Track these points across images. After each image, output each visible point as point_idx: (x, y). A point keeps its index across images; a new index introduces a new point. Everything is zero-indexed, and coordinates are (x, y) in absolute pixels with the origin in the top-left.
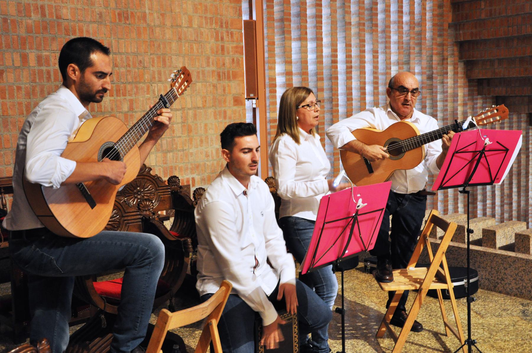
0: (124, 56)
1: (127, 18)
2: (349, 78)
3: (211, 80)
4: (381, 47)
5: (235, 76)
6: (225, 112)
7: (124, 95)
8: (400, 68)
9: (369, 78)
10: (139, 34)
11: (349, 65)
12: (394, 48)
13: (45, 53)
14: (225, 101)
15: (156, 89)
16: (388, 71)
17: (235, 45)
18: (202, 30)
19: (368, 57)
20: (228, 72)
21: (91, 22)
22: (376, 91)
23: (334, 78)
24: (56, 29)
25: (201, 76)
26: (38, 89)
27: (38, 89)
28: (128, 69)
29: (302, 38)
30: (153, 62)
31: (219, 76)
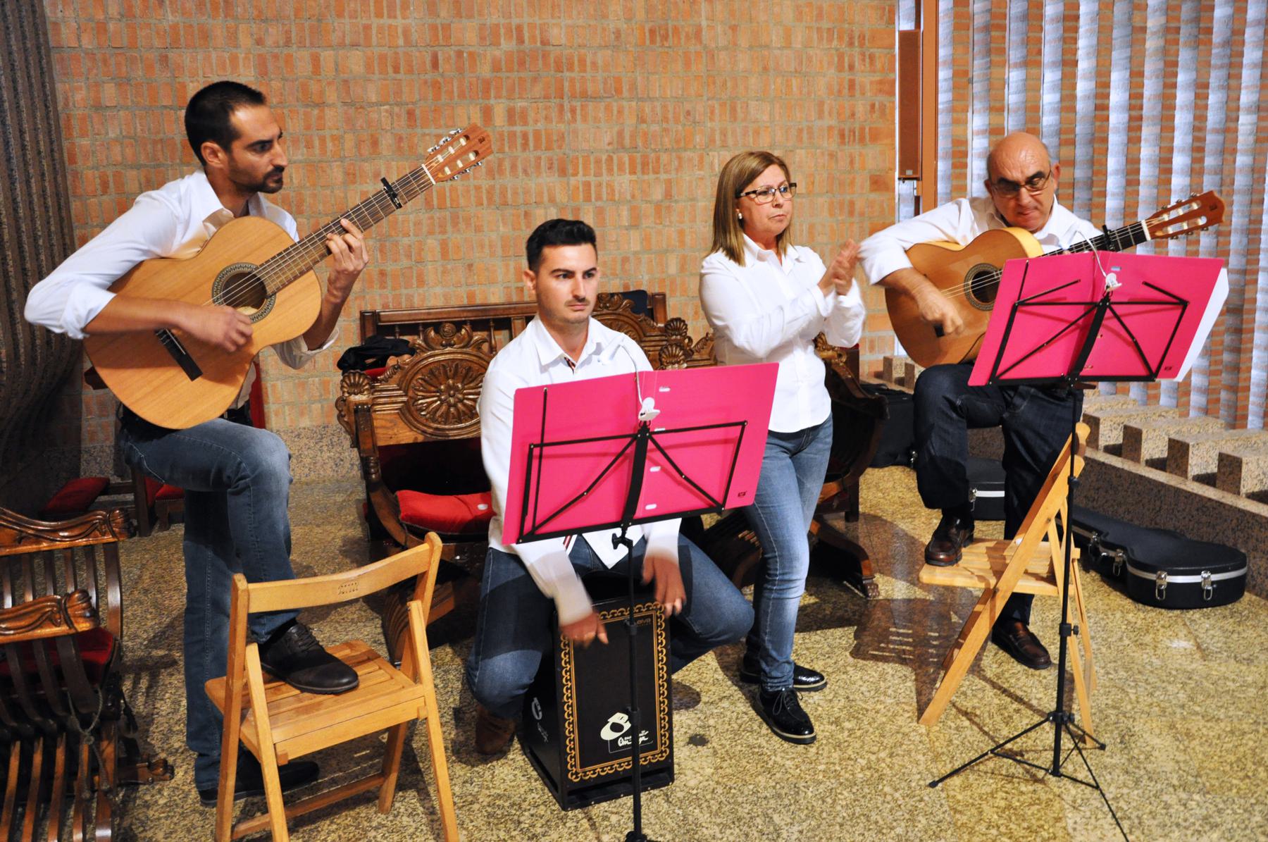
0: (658, 104)
1: (665, 37)
2: (1133, 137)
3: (825, 145)
4: (1216, 78)
5: (875, 136)
6: (852, 203)
7: (656, 172)
8: (1260, 119)
9: (1181, 138)
10: (687, 64)
11: (1134, 113)
12: (1249, 76)
13: (520, 104)
14: (852, 183)
15: (716, 161)
16: (1232, 125)
17: (877, 77)
18: (811, 52)
19: (1183, 97)
20: (862, 129)
21: (600, 47)
22: (1197, 166)
23: (1099, 140)
24: (540, 62)
25: (805, 136)
26: (507, 165)
27: (507, 165)
28: (665, 125)
29: (1032, 61)
30: (712, 112)
31: (842, 136)
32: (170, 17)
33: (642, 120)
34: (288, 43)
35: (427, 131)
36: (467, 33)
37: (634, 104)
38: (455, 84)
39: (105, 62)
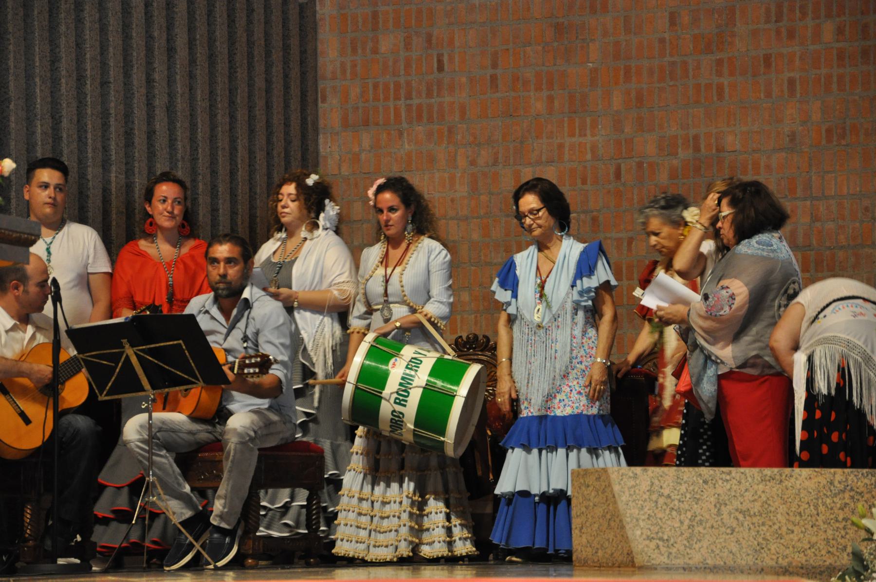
28: (841, 222)
32: (407, 146)
33: (815, 218)
34: (495, 162)
35: (608, 235)
36: (648, 145)
37: (808, 203)
38: (636, 192)
39: (356, 185)
